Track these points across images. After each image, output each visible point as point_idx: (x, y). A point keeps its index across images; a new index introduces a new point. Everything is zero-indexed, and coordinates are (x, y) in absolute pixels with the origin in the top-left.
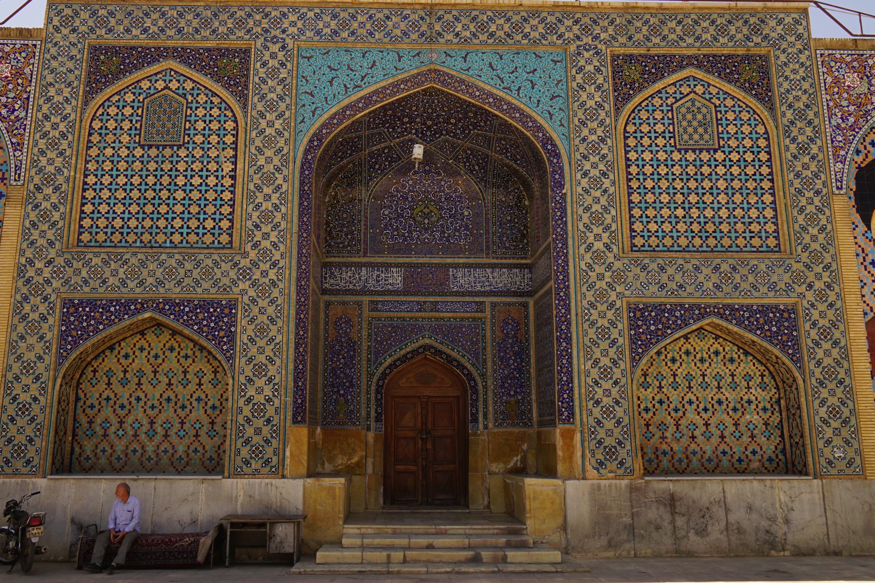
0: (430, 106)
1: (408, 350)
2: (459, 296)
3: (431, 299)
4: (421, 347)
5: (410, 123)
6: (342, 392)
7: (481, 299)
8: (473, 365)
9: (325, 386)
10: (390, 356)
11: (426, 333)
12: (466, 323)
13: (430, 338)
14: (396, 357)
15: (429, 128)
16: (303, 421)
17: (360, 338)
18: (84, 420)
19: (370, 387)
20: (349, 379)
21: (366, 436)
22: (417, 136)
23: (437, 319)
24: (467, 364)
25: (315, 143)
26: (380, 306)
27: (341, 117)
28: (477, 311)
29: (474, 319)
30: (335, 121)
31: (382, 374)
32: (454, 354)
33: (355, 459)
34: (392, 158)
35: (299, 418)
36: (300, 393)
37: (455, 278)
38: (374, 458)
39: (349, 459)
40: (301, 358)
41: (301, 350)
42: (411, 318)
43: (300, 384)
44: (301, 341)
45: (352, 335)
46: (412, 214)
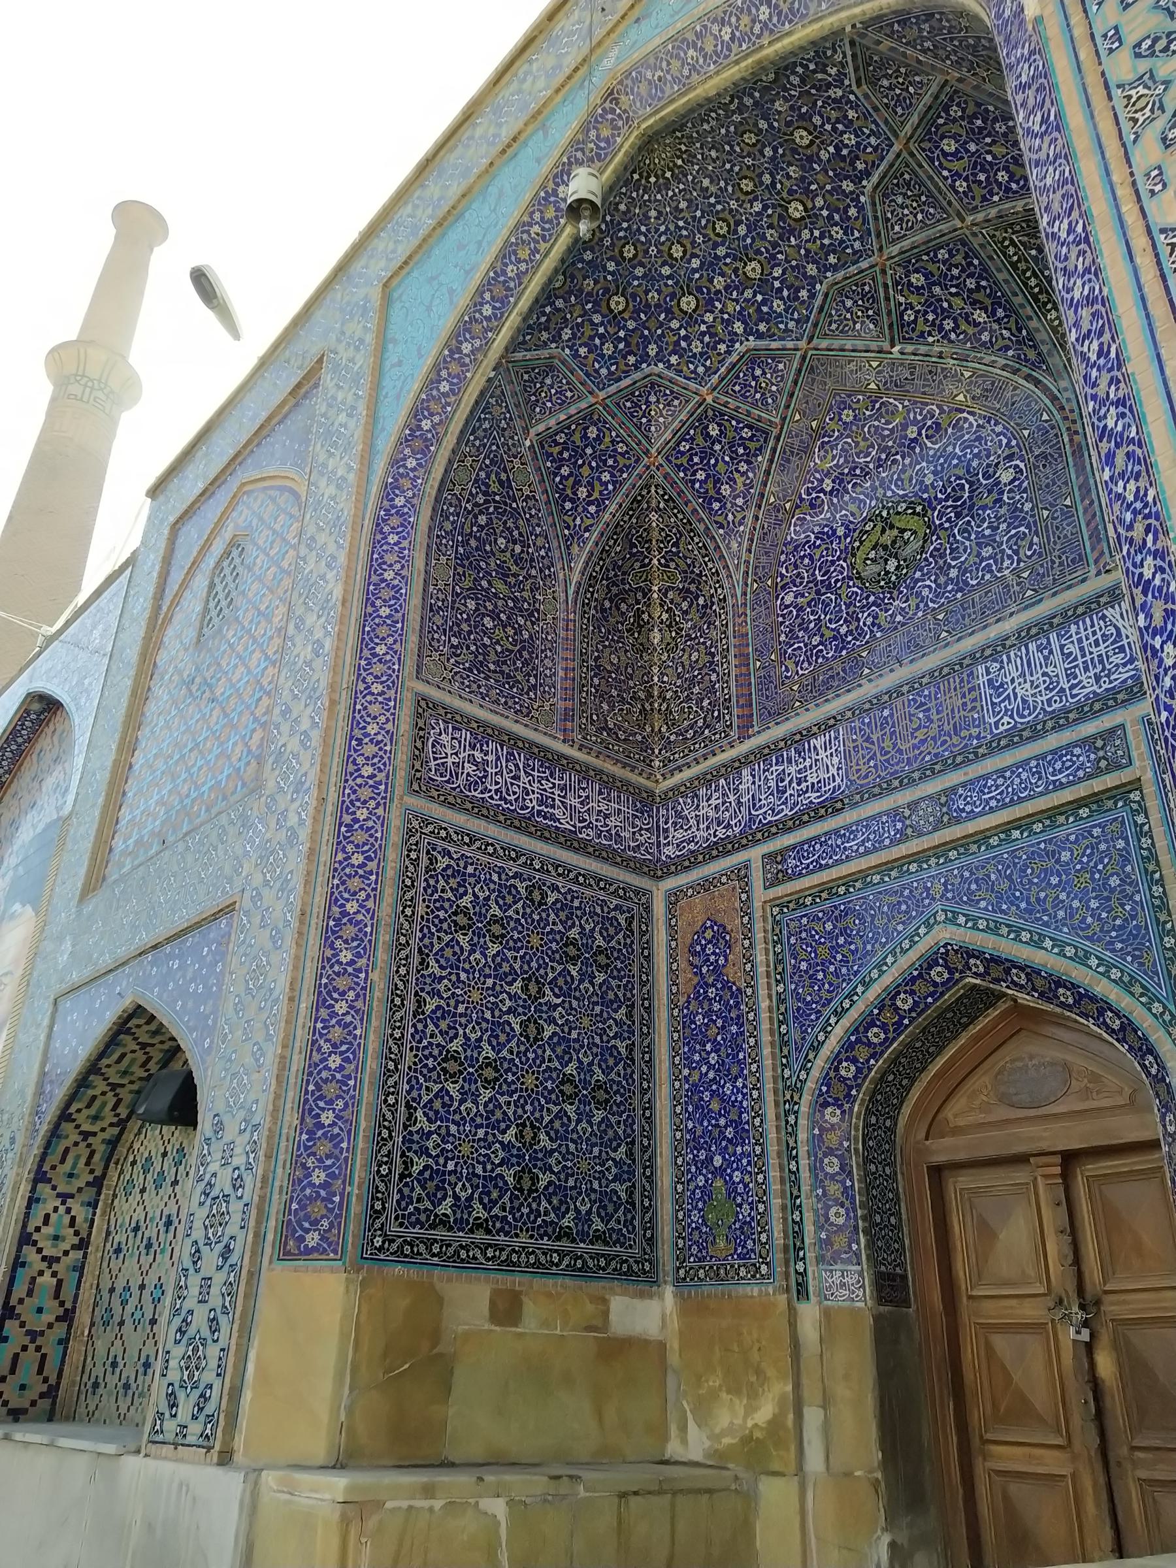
0: (709, 211)
1: (887, 979)
2: (1023, 741)
3: (932, 787)
4: (931, 963)
5: (709, 306)
6: (718, 1161)
7: (1106, 722)
8: (1127, 986)
9: (677, 1152)
10: (840, 1014)
11: (938, 906)
12: (1068, 829)
13: (953, 921)
14: (854, 1014)
15: (764, 283)
16: (328, 1247)
17: (752, 976)
18: (106, 1285)
19: (793, 1134)
20: (734, 1116)
21: (792, 1312)
22: (760, 336)
23: (961, 844)
24: (1103, 988)
25: (411, 463)
26: (792, 862)
27: (454, 368)
28: (1098, 772)
29: (1094, 800)
30: (445, 387)
31: (826, 1081)
32: (1045, 959)
33: (765, 1413)
34: (743, 442)
35: (312, 1239)
36: (323, 1148)
37: (999, 688)
38: (824, 1407)
39: (750, 1410)
40: (337, 1033)
41: (341, 1007)
42: (884, 868)
43: (327, 1118)
44: (342, 983)
45: (731, 973)
46: (852, 566)
